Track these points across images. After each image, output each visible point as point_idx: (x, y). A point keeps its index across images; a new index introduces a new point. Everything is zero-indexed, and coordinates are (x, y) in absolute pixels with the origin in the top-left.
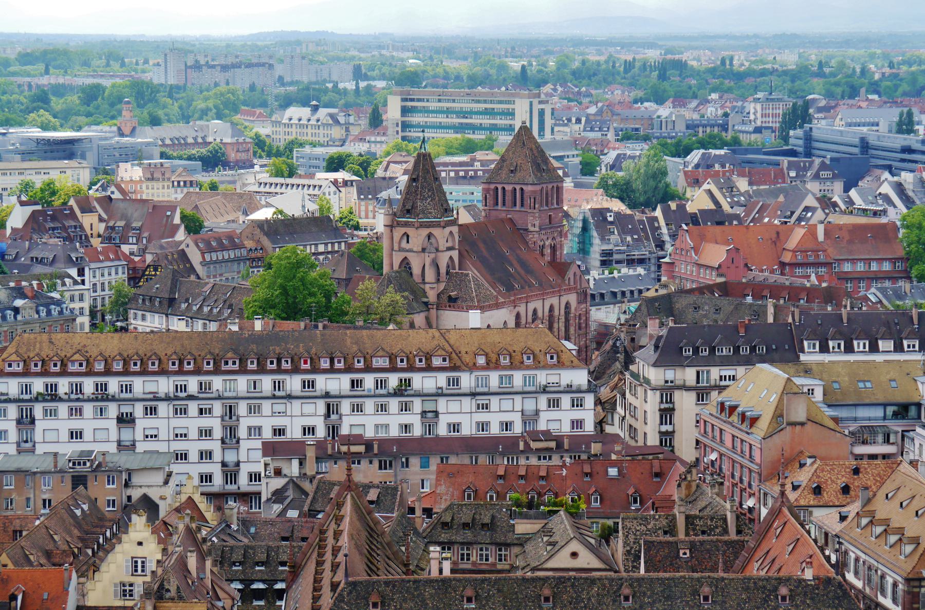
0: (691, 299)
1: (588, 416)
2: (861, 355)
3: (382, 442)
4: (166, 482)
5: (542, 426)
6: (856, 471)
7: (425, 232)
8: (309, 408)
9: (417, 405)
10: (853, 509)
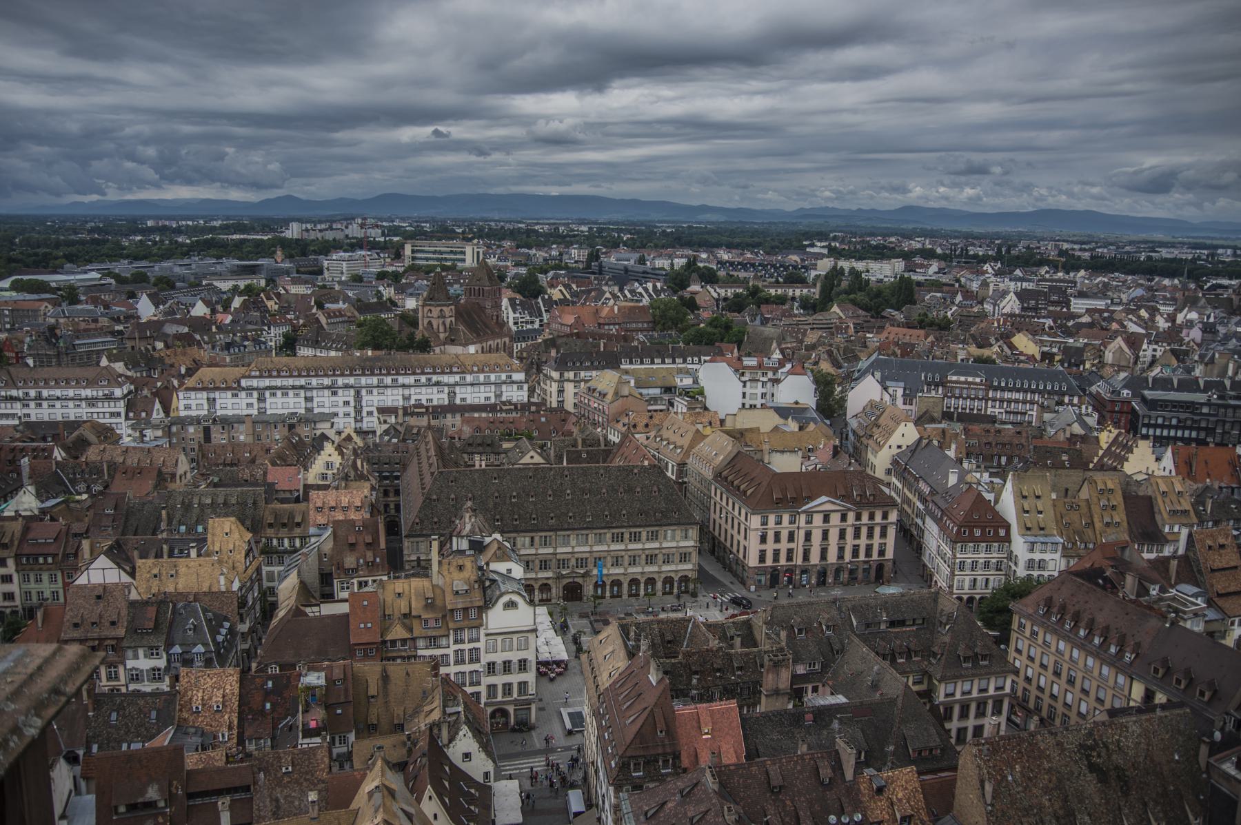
0: (564, 339)
1: (525, 394)
2: (647, 366)
3: (433, 407)
5: (504, 399)
6: (651, 417)
7: (439, 308)
8: (395, 392)
9: (446, 390)
10: (652, 434)
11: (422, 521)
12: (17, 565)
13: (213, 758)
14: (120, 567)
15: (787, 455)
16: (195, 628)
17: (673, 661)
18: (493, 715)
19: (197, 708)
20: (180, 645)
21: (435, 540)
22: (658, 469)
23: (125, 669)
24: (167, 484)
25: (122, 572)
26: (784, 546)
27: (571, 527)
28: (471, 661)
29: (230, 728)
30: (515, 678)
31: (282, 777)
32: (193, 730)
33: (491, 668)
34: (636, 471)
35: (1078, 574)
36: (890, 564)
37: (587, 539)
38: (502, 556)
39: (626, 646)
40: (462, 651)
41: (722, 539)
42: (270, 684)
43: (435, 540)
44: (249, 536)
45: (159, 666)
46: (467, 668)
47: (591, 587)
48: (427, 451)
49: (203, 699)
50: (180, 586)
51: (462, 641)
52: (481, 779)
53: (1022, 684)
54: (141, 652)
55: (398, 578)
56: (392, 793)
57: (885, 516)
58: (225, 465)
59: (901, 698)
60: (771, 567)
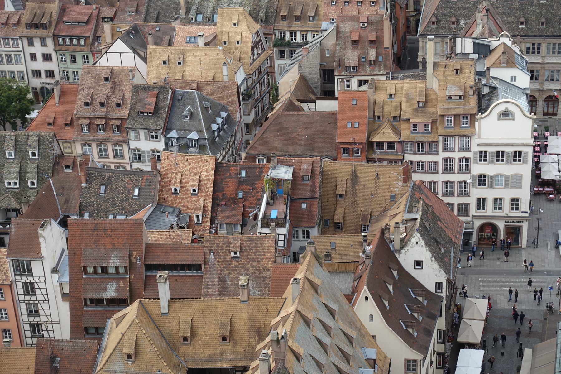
11: (438, 21)
12: (55, 45)
14: (135, 51)
16: (191, 115)
18: (482, 228)
19: (176, 190)
20: (177, 130)
21: (431, 40)
23: (129, 148)
25: (136, 57)
28: (461, 171)
29: (204, 211)
30: (507, 195)
31: (231, 261)
32: (171, 210)
33: (482, 180)
40: (452, 159)
42: (243, 174)
43: (431, 40)
44: (257, 27)
45: (158, 149)
46: (456, 177)
49: (181, 182)
50: (187, 74)
51: (453, 150)
52: (432, 289)
54: (142, 133)
55: (396, 78)
56: (315, 288)
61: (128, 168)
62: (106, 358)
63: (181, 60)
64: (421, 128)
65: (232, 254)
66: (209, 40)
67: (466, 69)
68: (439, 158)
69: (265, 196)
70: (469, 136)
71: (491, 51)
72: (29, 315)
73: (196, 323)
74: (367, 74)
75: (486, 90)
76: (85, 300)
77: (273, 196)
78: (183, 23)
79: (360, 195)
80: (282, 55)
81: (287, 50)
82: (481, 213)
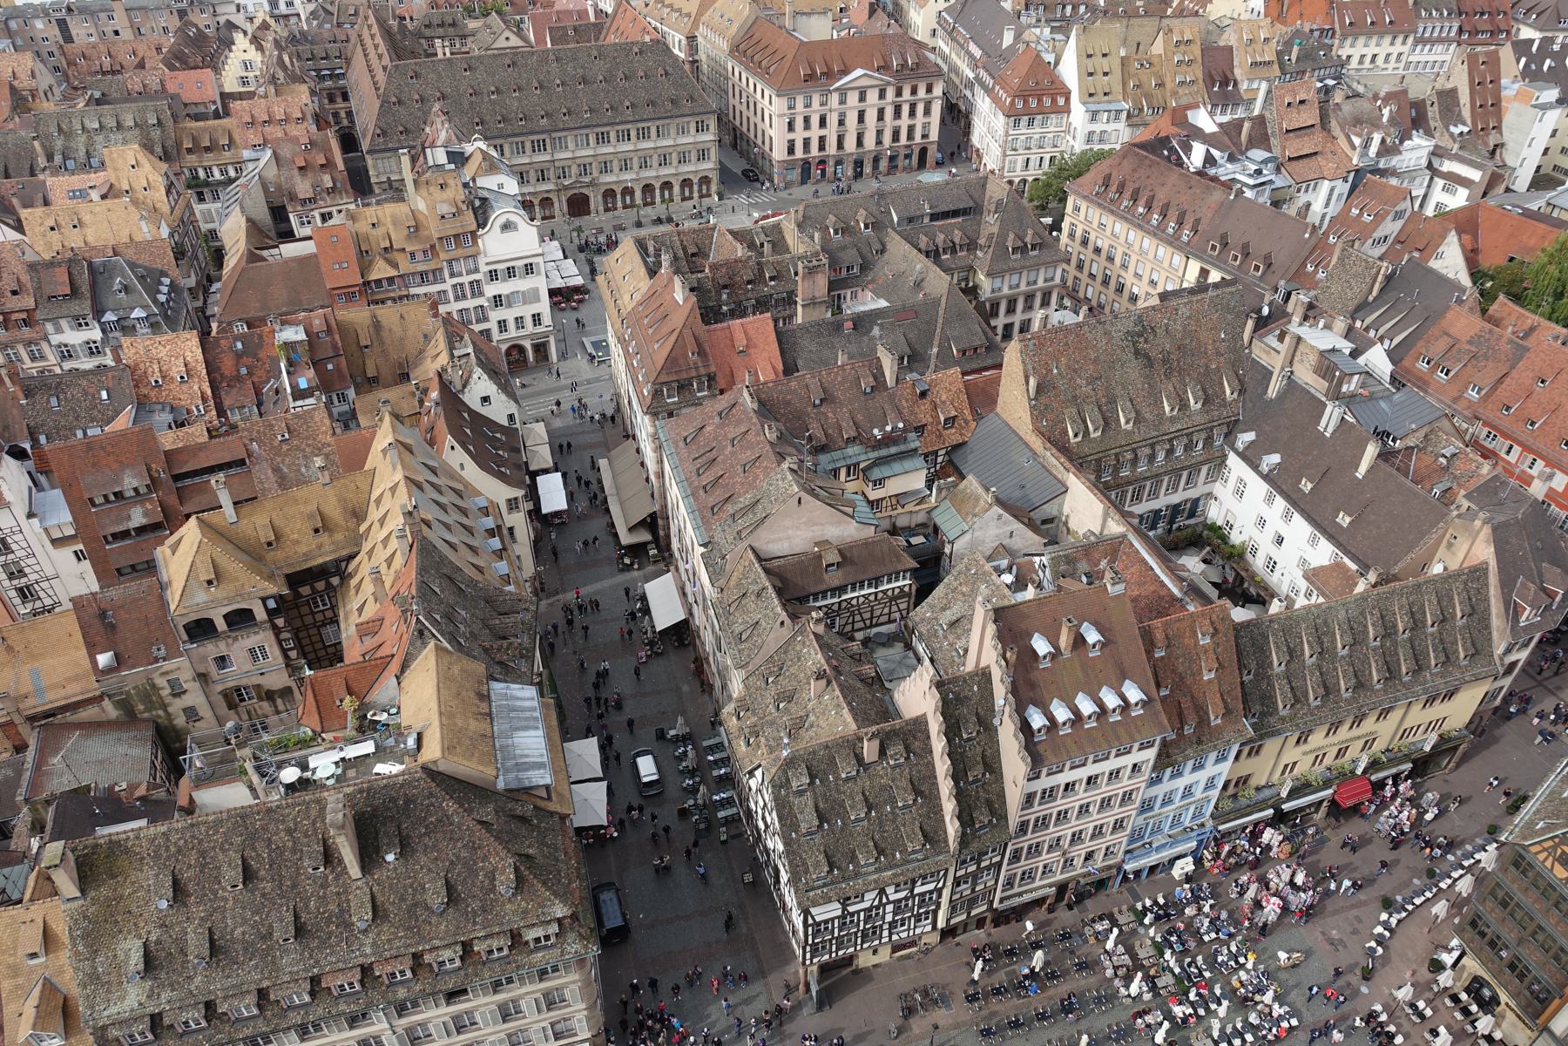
4: (238, 11)
11: (384, 133)
13: (193, 434)
15: (814, 20)
16: (126, 289)
17: (699, 275)
18: (508, 352)
19: (156, 382)
20: (113, 310)
22: (661, 46)
23: (51, 346)
24: (30, 105)
26: (815, 133)
27: (567, 126)
28: (474, 296)
29: (204, 399)
30: (527, 311)
32: (160, 407)
33: (498, 301)
34: (636, 50)
35: (1142, 146)
36: (935, 146)
37: (588, 140)
38: (491, 167)
39: (645, 262)
40: (461, 285)
41: (744, 129)
42: (239, 345)
44: (164, 166)
45: (94, 338)
46: (470, 303)
47: (600, 198)
48: (373, 36)
49: (161, 371)
50: (90, 239)
51: (460, 275)
53: (1072, 270)
54: (64, 323)
55: (368, 205)
56: (409, 448)
57: (929, 90)
58: (104, 73)
59: (945, 297)
60: (802, 160)
61: (58, 371)
62: (179, 592)
63: (76, 222)
64: (419, 256)
65: (280, 438)
66: (104, 191)
67: (451, 182)
68: (449, 283)
69: (282, 365)
70: (474, 256)
71: (467, 159)
72: (10, 579)
73: (277, 523)
74: (326, 204)
75: (477, 203)
76: (105, 537)
77: (290, 363)
78: (52, 175)
79: (388, 342)
80: (201, 199)
81: (205, 190)
82: (505, 336)
